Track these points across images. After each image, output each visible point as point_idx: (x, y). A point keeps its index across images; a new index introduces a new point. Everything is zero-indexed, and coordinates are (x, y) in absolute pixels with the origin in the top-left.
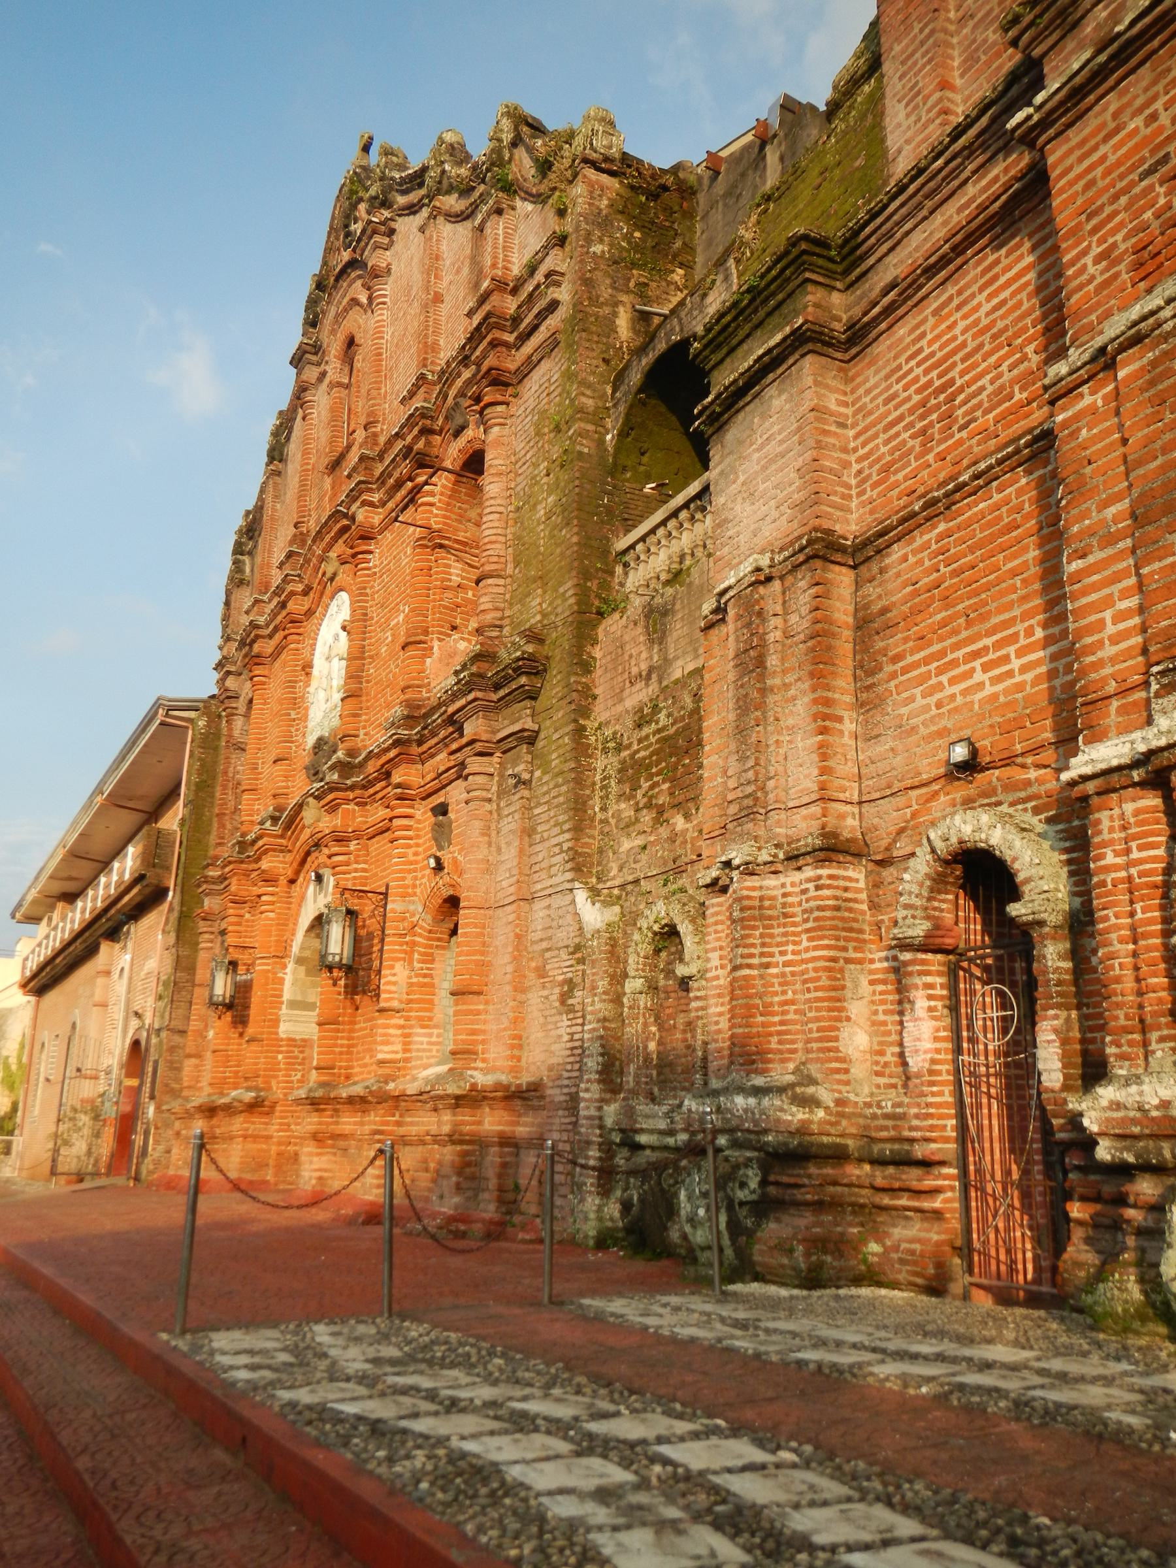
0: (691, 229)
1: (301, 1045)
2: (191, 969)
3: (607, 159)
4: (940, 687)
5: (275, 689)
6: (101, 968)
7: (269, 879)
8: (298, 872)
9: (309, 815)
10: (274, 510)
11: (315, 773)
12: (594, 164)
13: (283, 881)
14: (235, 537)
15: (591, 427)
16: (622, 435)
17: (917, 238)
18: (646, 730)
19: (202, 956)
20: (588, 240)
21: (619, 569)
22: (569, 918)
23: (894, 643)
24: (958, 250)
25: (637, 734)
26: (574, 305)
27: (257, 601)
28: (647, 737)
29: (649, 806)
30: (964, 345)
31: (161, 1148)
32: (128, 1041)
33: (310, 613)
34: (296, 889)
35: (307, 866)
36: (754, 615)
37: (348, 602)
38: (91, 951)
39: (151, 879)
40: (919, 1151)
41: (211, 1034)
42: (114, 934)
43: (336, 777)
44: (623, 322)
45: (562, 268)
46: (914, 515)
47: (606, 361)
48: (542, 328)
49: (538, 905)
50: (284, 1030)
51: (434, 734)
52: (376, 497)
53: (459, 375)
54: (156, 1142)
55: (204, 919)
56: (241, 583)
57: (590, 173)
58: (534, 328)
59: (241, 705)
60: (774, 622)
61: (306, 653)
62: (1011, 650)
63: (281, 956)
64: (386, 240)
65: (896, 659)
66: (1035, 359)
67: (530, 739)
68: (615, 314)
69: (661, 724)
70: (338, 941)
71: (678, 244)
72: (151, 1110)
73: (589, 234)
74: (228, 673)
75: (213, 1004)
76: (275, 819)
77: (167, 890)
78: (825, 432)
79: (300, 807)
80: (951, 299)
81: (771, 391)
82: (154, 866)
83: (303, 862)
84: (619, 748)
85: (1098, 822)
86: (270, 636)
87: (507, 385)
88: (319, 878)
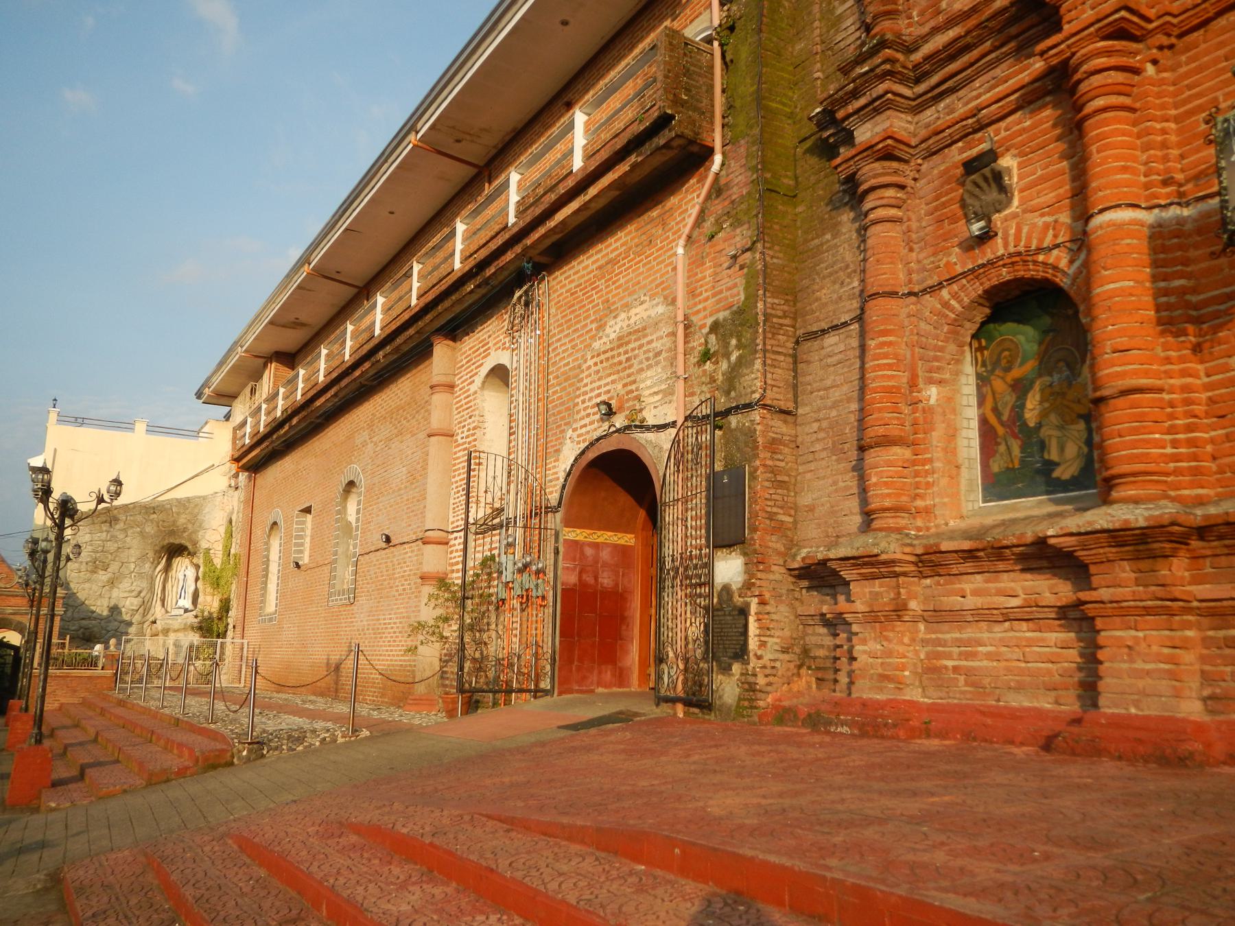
6: (435, 380)
38: (422, 352)
39: (679, 125)
42: (457, 329)
55: (888, 156)
77: (710, 152)
82: (683, 104)
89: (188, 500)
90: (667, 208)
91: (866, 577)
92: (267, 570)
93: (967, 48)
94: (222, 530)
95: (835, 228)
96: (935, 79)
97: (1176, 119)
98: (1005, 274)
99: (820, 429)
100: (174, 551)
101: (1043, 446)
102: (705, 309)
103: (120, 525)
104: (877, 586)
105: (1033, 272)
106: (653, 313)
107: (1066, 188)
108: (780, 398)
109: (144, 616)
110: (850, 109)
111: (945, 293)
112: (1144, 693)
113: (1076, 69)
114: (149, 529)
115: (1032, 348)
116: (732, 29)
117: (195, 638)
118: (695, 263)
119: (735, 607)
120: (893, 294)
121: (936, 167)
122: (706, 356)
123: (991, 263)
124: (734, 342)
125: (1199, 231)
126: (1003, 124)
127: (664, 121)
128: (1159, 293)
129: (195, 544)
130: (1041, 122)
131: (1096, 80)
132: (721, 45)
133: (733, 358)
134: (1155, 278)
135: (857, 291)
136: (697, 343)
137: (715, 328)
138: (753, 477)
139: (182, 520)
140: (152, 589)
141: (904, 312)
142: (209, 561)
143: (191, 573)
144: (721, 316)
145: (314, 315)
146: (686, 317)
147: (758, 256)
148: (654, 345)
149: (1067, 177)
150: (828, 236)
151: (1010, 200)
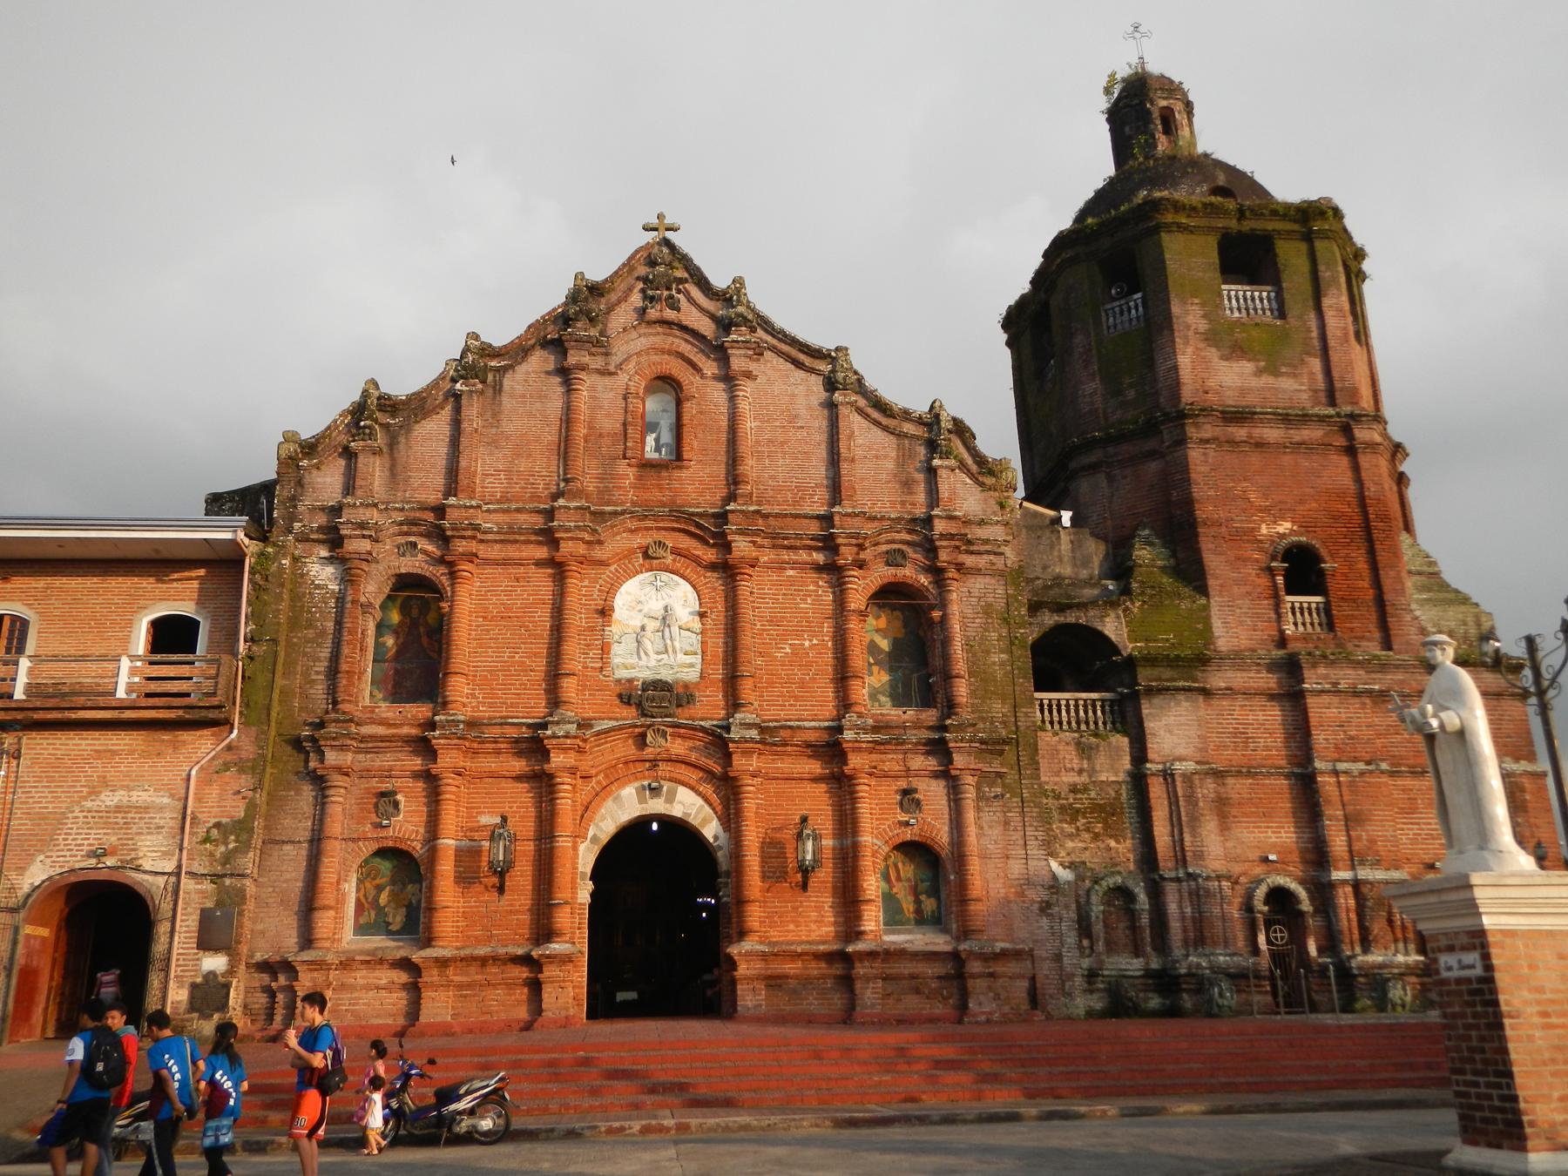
4: (1254, 832)
17: (1230, 674)
23: (1234, 811)
24: (1255, 694)
25: (1071, 795)
26: (1020, 567)
28: (1081, 799)
29: (1088, 830)
30: (1252, 724)
33: (602, 563)
40: (1262, 974)
46: (1241, 772)
48: (985, 557)
51: (902, 744)
53: (897, 532)
56: (377, 452)
58: (979, 553)
62: (1282, 831)
65: (1235, 817)
66: (1280, 744)
67: (999, 775)
69: (1092, 796)
76: (580, 726)
80: (1246, 705)
85: (1337, 892)
86: (482, 541)
90: (181, 738)
91: (311, 970)
93: (391, 741)
95: (298, 792)
96: (370, 745)
97: (467, 808)
98: (391, 844)
99: (273, 891)
101: (386, 915)
102: (209, 812)
104: (315, 974)
105: (403, 847)
106: (158, 800)
107: (425, 818)
110: (328, 743)
111: (361, 843)
112: (437, 1014)
113: (440, 779)
115: (389, 873)
116: (251, 658)
118: (205, 781)
119: (219, 984)
120: (336, 838)
121: (364, 784)
122: (206, 840)
123: (386, 838)
124: (233, 837)
125: (468, 852)
126: (400, 780)
127: (219, 707)
128: (455, 872)
130: (417, 787)
131: (449, 788)
132: (243, 666)
133: (231, 846)
134: (455, 866)
135: (310, 828)
136: (201, 831)
137: (217, 825)
138: (241, 914)
141: (339, 847)
144: (224, 820)
146: (192, 813)
147: (258, 796)
148: (156, 821)
149: (425, 814)
150: (293, 793)
151: (398, 815)
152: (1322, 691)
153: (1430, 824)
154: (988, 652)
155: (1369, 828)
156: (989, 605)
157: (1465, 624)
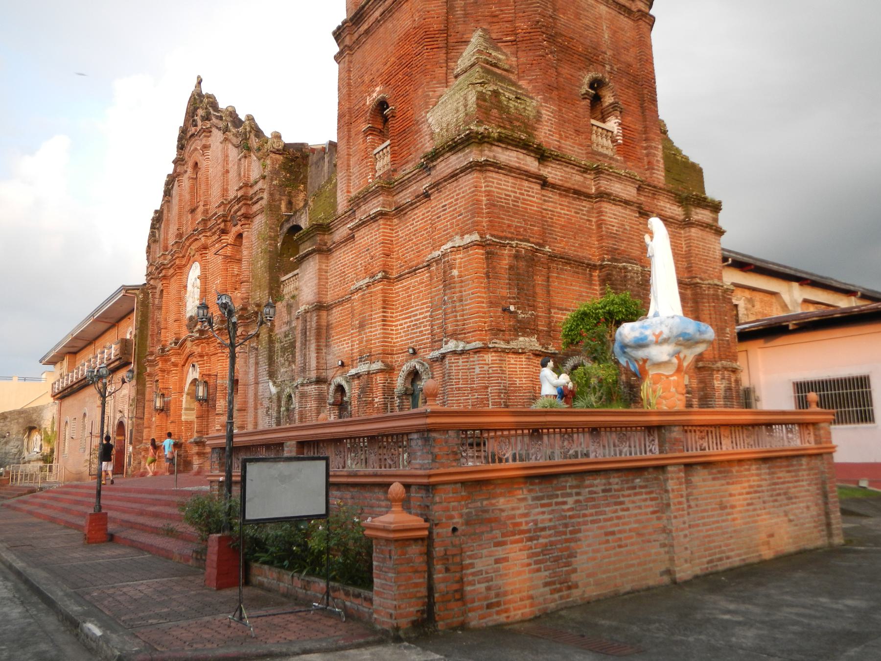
0: (306, 171)
1: (189, 423)
2: (143, 394)
3: (278, 150)
5: (173, 286)
7: (175, 365)
8: (185, 363)
9: (189, 344)
10: (168, 216)
11: (190, 328)
12: (274, 152)
13: (180, 365)
14: (151, 222)
15: (273, 242)
16: (283, 244)
17: (341, 230)
18: (287, 339)
19: (148, 390)
20: (272, 180)
21: (282, 286)
22: (268, 390)
24: (346, 241)
27: (163, 255)
29: (287, 360)
31: (136, 462)
32: (116, 422)
33: (185, 266)
34: (185, 369)
35: (189, 361)
36: (305, 321)
37: (199, 268)
41: (154, 419)
43: (198, 335)
44: (283, 206)
45: (265, 187)
47: (278, 220)
49: (260, 385)
50: (183, 418)
52: (208, 234)
54: (134, 460)
56: (155, 241)
57: (272, 155)
59: (158, 291)
60: (308, 323)
61: (184, 280)
63: (181, 392)
64: (209, 134)
65: (333, 337)
68: (281, 204)
70: (201, 392)
71: (302, 176)
72: (131, 449)
73: (272, 177)
74: (152, 278)
75: (156, 410)
76: (176, 343)
78: (321, 275)
79: (185, 340)
81: (311, 259)
83: (187, 359)
84: (281, 342)
87: (249, 218)
88: (194, 366)
89: (37, 407)
92: (65, 438)
94: (51, 420)
100: (31, 429)
103: (9, 420)
108: (139, 415)
109: (20, 455)
114: (21, 420)
117: (41, 464)
127: (120, 358)
129: (40, 426)
139: (34, 416)
140: (23, 445)
142: (46, 433)
143: (39, 437)
145: (81, 344)
152: (358, 226)
153: (416, 315)
154: (258, 261)
155: (367, 331)
156: (259, 232)
157: (458, 111)
